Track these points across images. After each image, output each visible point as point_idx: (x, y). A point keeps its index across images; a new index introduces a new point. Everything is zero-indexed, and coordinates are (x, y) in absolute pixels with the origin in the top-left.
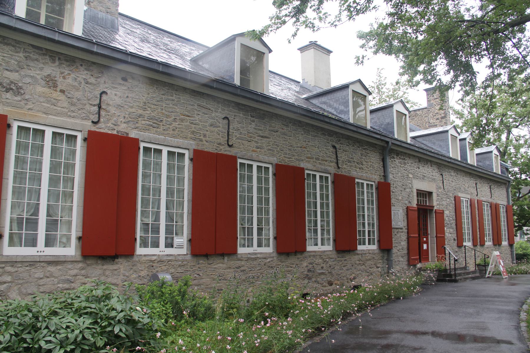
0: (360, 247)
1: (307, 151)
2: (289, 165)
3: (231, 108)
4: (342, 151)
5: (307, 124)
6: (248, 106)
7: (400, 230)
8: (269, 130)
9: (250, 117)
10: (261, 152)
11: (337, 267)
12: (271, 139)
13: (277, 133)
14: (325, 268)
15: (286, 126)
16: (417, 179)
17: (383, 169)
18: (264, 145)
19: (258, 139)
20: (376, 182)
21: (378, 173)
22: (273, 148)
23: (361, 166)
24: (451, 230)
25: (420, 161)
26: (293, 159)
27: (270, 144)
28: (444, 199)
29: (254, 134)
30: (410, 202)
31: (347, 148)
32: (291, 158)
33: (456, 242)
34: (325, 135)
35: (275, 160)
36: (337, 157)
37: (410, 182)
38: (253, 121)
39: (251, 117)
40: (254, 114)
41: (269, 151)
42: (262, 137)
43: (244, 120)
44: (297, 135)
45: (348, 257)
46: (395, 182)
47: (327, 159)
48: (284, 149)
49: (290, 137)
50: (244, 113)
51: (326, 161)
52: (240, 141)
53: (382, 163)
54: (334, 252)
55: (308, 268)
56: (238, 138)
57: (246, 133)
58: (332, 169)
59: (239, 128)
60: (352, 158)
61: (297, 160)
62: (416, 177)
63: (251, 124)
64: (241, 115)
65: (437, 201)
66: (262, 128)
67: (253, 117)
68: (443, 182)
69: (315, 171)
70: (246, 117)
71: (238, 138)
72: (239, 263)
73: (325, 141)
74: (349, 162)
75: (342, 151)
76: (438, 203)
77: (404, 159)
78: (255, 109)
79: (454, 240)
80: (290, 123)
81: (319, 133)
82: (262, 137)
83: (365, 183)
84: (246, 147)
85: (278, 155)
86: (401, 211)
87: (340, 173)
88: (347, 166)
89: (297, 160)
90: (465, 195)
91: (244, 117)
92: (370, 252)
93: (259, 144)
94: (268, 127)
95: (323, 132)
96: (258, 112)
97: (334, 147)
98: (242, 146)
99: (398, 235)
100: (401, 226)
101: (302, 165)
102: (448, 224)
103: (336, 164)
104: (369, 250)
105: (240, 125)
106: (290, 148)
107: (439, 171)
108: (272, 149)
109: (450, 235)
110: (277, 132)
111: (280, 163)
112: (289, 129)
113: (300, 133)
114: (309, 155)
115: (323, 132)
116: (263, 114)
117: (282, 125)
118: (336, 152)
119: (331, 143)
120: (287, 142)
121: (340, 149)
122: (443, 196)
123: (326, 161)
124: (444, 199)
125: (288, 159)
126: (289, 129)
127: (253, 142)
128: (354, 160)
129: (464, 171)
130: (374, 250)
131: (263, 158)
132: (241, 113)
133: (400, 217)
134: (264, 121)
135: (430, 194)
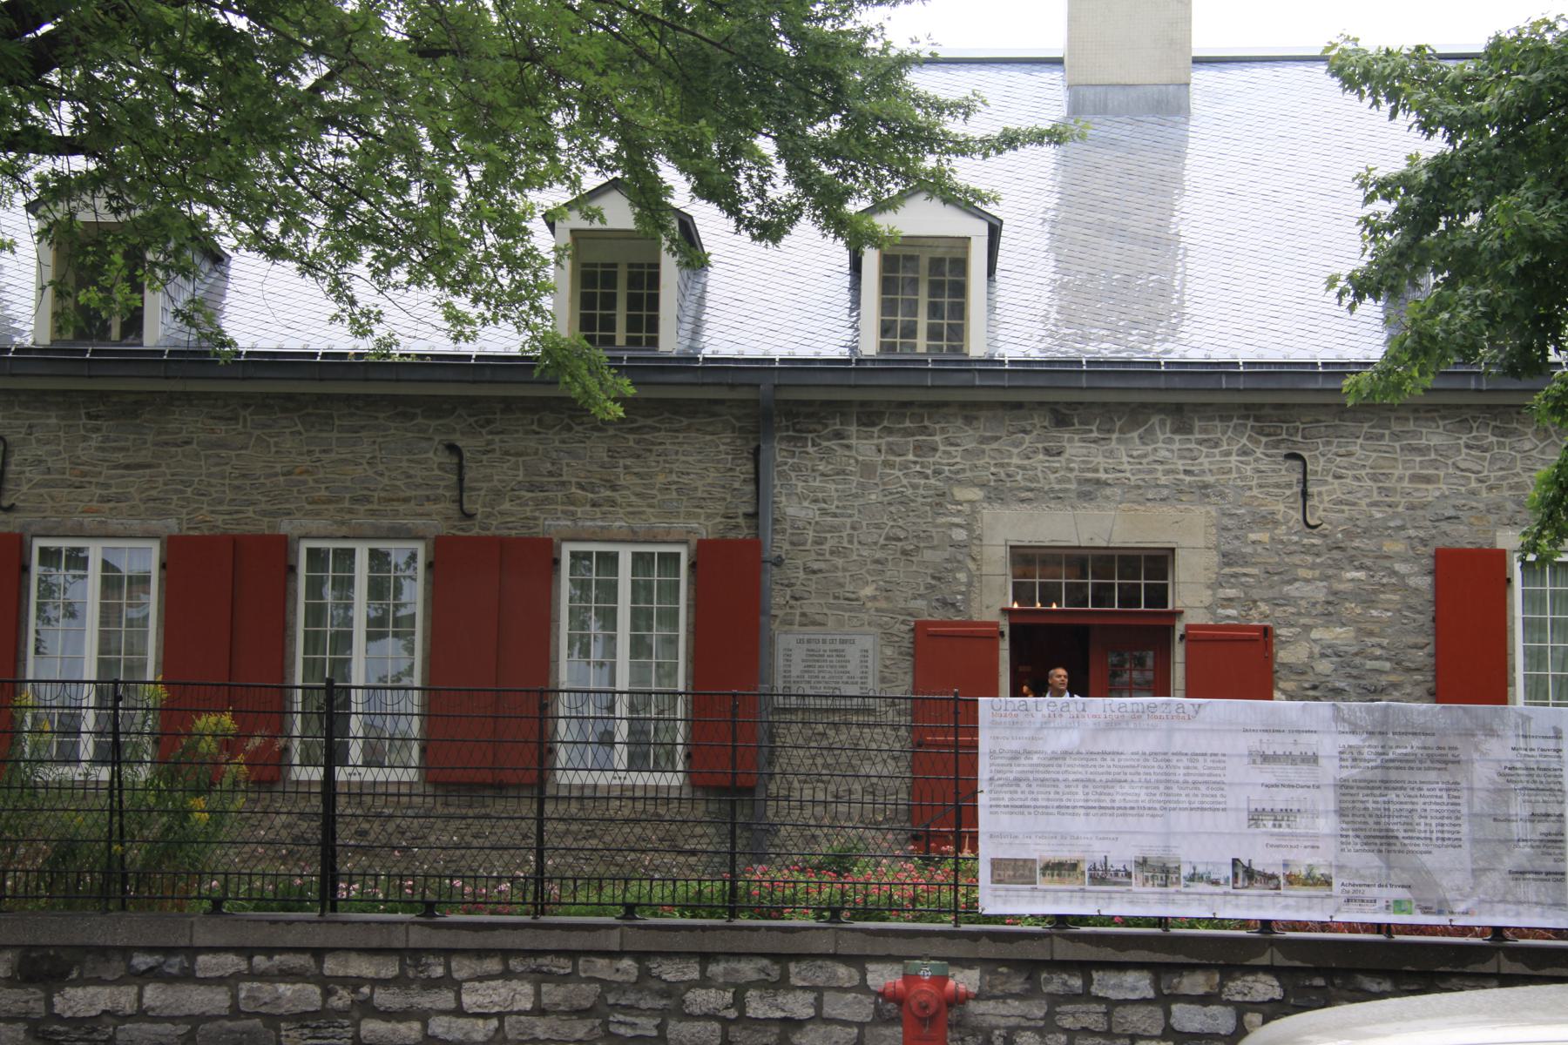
1: (316, 481)
2: (230, 532)
3: (17, 409)
4: (498, 454)
5: (322, 399)
6: (77, 391)
8: (156, 444)
9: (84, 421)
10: (114, 513)
12: (163, 469)
13: (187, 447)
15: (230, 419)
16: (1023, 501)
17: (750, 488)
18: (132, 490)
19: (111, 477)
20: (693, 542)
22: (166, 492)
23: (608, 493)
26: (251, 515)
27: (155, 482)
28: (1302, 573)
29: (95, 466)
30: (945, 603)
31: (532, 443)
32: (237, 512)
35: (172, 526)
36: (461, 480)
38: (98, 430)
39: (89, 416)
40: (102, 408)
41: (151, 504)
42: (127, 467)
43: (61, 434)
44: (272, 441)
47: (409, 493)
48: (212, 490)
49: (241, 448)
50: (62, 413)
51: (406, 500)
52: (43, 491)
53: (750, 467)
55: (296, 831)
56: (38, 485)
57: (67, 465)
59: (44, 458)
60: (551, 474)
61: (265, 513)
62: (998, 493)
63: (85, 439)
64: (53, 421)
65: (1219, 584)
66: (129, 444)
67: (97, 417)
68: (1305, 495)
69: (345, 537)
70: (70, 422)
71: (38, 485)
73: (410, 435)
74: (532, 487)
75: (498, 454)
76: (1231, 593)
77: (924, 430)
78: (103, 396)
80: (246, 406)
81: (382, 415)
82: (127, 467)
84: (63, 503)
85: (185, 511)
87: (475, 531)
88: (520, 505)
89: (265, 513)
91: (63, 423)
93: (114, 490)
94: (150, 438)
95: (400, 409)
96: (115, 399)
97: (452, 448)
98: (50, 503)
101: (285, 527)
103: (455, 506)
105: (48, 447)
106: (236, 483)
107: (1276, 445)
108: (161, 496)
110: (187, 443)
111: (192, 533)
112: (240, 427)
113: (287, 430)
114: (324, 493)
115: (400, 409)
116: (136, 402)
117: (211, 421)
118: (460, 467)
119: (437, 439)
120: (228, 469)
121: (486, 452)
122: (1296, 559)
123: (406, 500)
124: (1302, 573)
125: (226, 517)
126: (240, 427)
127: (93, 488)
128: (564, 478)
131: (121, 527)
132: (53, 414)
134: (138, 421)
135: (1159, 562)
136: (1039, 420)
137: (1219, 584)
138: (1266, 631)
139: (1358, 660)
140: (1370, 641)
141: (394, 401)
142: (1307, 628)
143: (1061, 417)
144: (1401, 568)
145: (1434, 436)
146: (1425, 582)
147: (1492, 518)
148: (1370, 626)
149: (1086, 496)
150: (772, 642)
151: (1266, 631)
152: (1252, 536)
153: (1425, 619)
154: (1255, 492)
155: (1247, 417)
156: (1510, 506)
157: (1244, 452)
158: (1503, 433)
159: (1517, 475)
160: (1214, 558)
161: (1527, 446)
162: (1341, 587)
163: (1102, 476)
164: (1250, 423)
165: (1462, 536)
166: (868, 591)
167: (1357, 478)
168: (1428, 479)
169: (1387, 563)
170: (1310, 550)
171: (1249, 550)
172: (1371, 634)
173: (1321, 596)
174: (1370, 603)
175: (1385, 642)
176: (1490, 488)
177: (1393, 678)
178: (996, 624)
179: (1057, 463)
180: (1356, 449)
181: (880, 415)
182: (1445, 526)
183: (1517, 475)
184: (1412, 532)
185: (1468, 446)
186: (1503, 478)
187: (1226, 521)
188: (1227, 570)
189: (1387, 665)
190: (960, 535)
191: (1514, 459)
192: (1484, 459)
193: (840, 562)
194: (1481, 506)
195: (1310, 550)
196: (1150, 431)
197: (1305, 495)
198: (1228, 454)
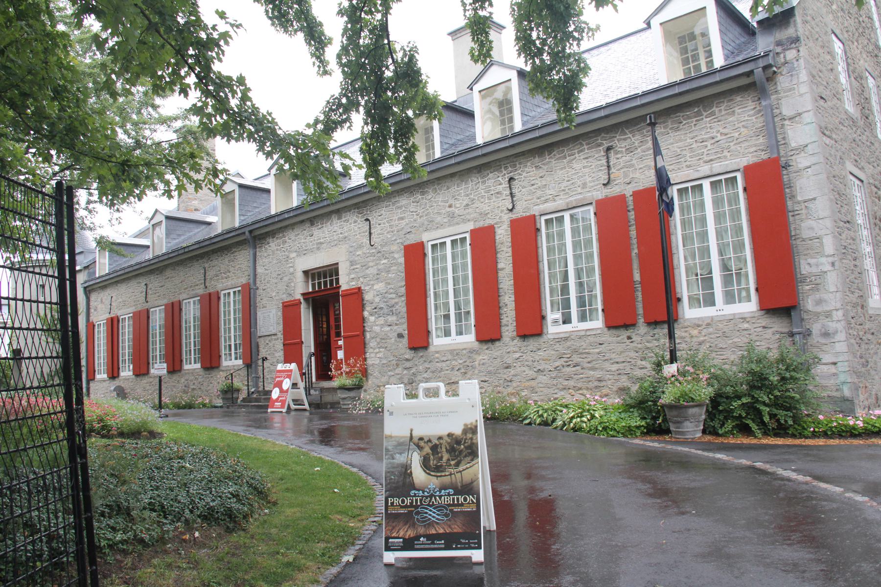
0: (186, 367)
7: (273, 337)
11: (205, 384)
14: (196, 384)
21: (246, 273)
24: (392, 319)
25: (312, 224)
33: (405, 341)
34: (198, 260)
35: (165, 301)
37: (291, 265)
45: (214, 373)
46: (267, 274)
54: (202, 370)
58: (201, 291)
65: (349, 274)
68: (370, 234)
72: (151, 380)
76: (353, 276)
79: (400, 336)
83: (231, 291)
86: (274, 311)
90: (451, 228)
92: (235, 368)
99: (271, 344)
100: (274, 332)
102: (381, 308)
104: (234, 366)
109: (387, 329)
122: (368, 259)
124: (371, 264)
129: (452, 175)
130: (239, 365)
133: (272, 321)
136: (308, 225)
137: (349, 274)
138: (359, 288)
139: (386, 295)
140: (389, 287)
141: (196, 256)
142: (373, 285)
143: (312, 221)
144: (396, 256)
145: (403, 201)
146: (402, 260)
147: (421, 229)
148: (388, 281)
149: (318, 249)
150: (256, 314)
151: (359, 288)
152: (358, 253)
153: (403, 275)
154: (358, 237)
155: (355, 209)
156: (426, 223)
157: (355, 222)
158: (423, 193)
159: (427, 209)
160: (348, 264)
161: (430, 197)
162: (380, 267)
163: (322, 240)
164: (356, 210)
165: (412, 240)
166: (274, 294)
167: (384, 224)
168: (402, 219)
169: (392, 255)
170: (373, 255)
171: (356, 259)
172: (389, 284)
173: (376, 272)
174: (388, 272)
175: (392, 286)
176: (421, 217)
177: (396, 300)
178: (300, 300)
179: (312, 239)
180: (383, 212)
181: (275, 234)
182: (407, 236)
183: (427, 209)
184: (398, 241)
185: (413, 202)
186: (423, 212)
187: (351, 249)
188: (352, 268)
189: (394, 296)
190: (291, 270)
191: (426, 203)
192: (417, 206)
193: (268, 285)
194: (417, 225)
195: (373, 255)
196: (332, 221)
197: (370, 234)
198: (351, 224)
